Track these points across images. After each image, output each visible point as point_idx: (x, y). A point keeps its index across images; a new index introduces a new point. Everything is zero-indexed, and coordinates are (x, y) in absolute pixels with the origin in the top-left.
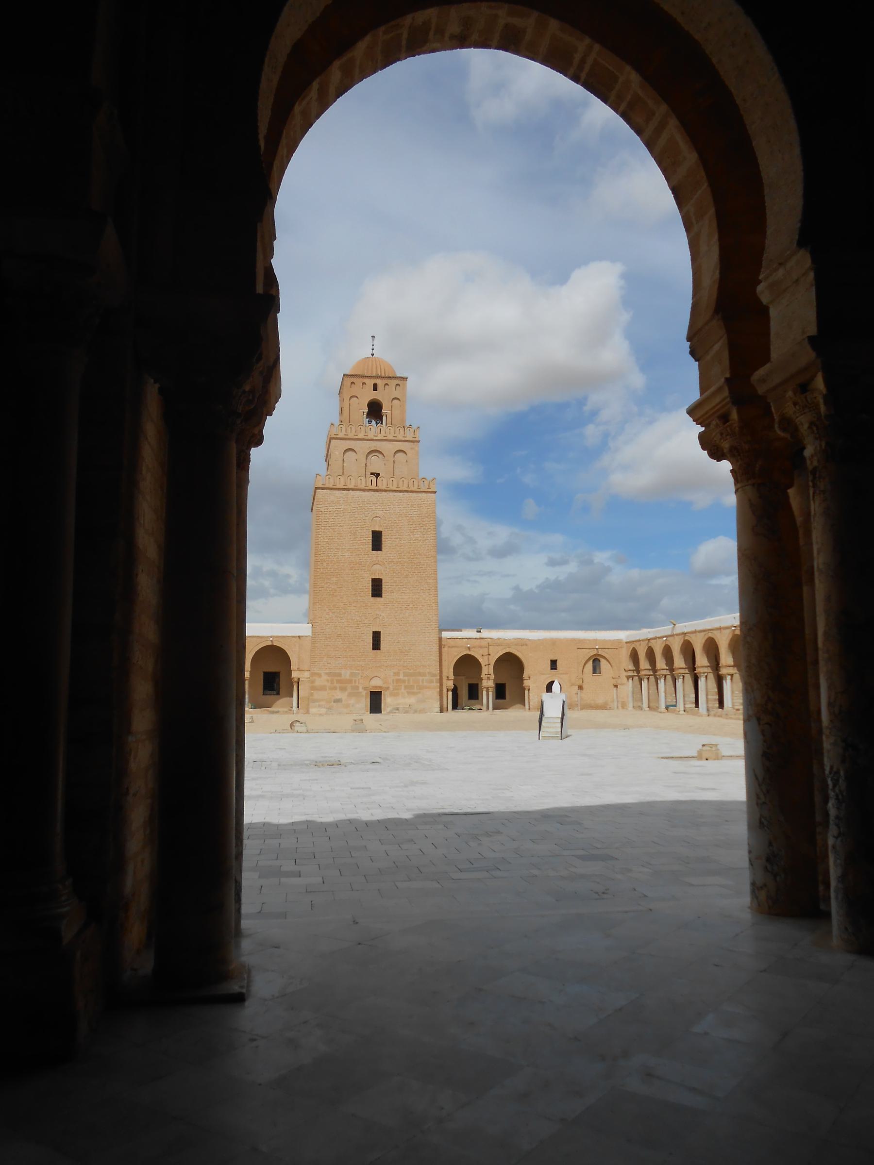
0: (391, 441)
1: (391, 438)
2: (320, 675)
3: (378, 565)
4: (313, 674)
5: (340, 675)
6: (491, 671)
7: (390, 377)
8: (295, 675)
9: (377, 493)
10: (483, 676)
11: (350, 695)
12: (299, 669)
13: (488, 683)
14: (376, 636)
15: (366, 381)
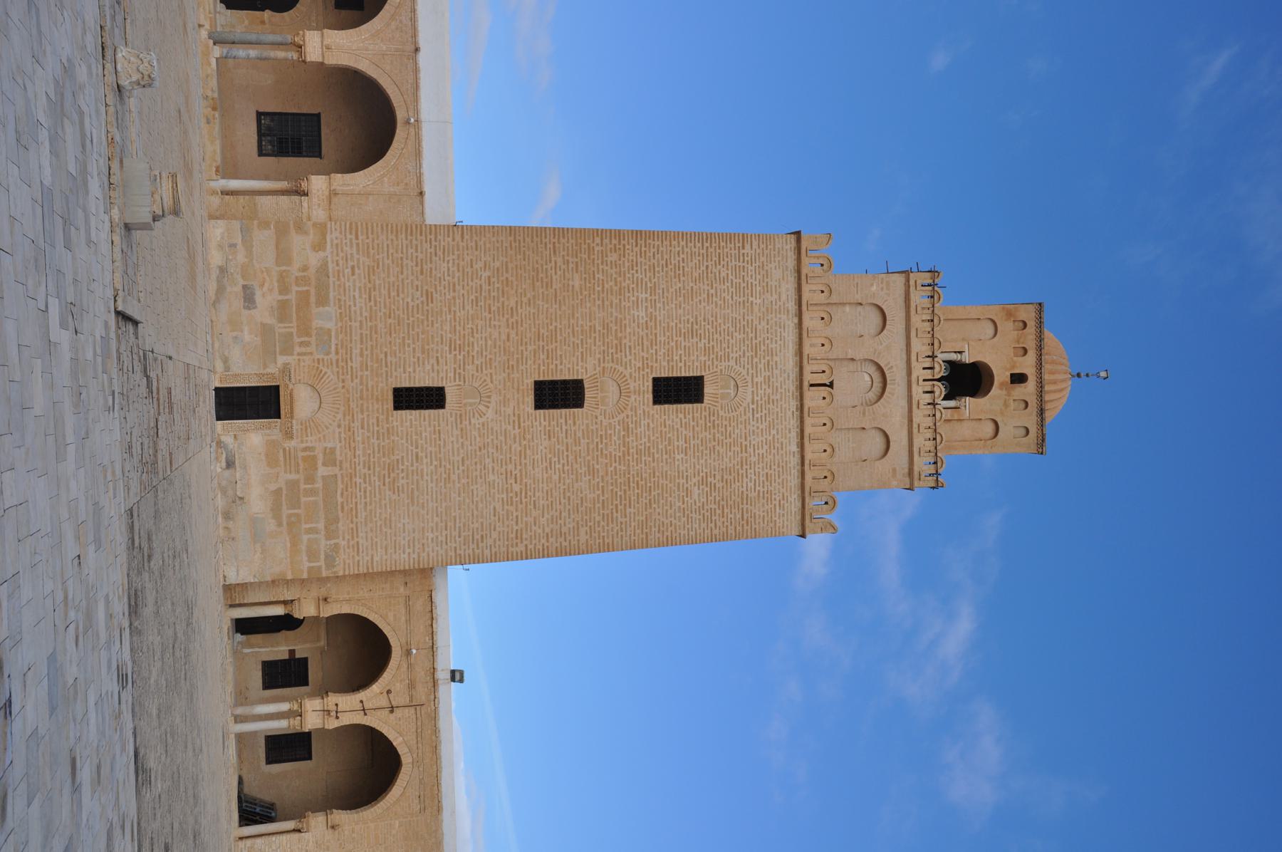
0: (910, 421)
1: (916, 420)
2: (319, 246)
3: (619, 396)
4: (322, 229)
5: (322, 301)
6: (346, 720)
7: (1041, 412)
8: (318, 183)
9: (791, 386)
10: (333, 699)
11: (266, 331)
12: (333, 194)
13: (316, 712)
14: (430, 398)
15: (1031, 357)
